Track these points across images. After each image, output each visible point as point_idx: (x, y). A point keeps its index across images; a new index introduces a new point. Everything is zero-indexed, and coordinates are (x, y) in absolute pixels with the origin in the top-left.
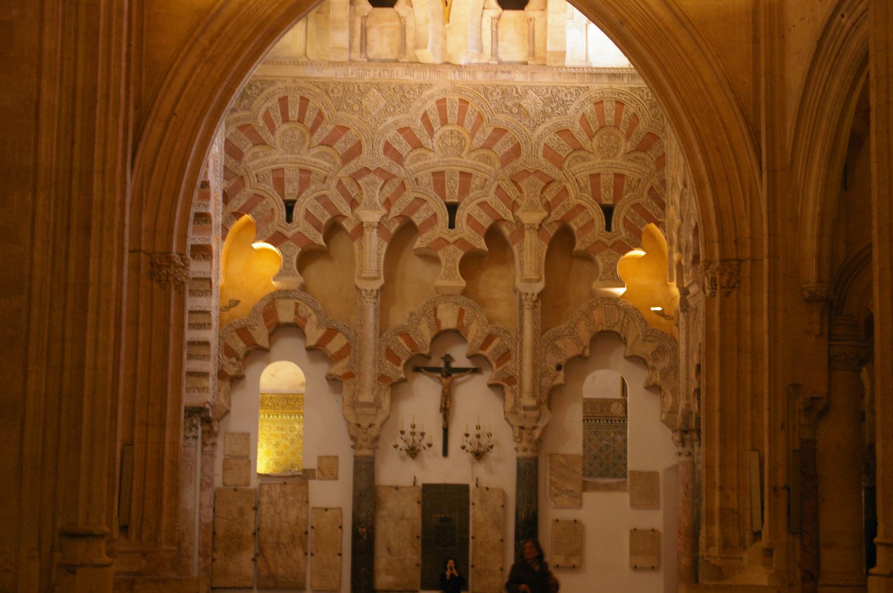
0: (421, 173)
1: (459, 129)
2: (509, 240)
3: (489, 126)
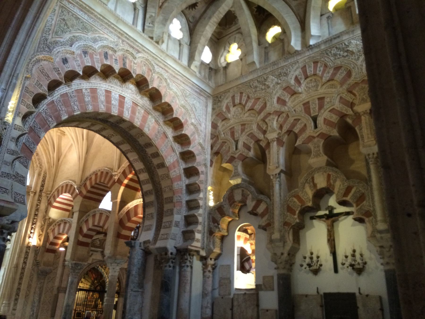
1: (315, 77)
2: (353, 125)
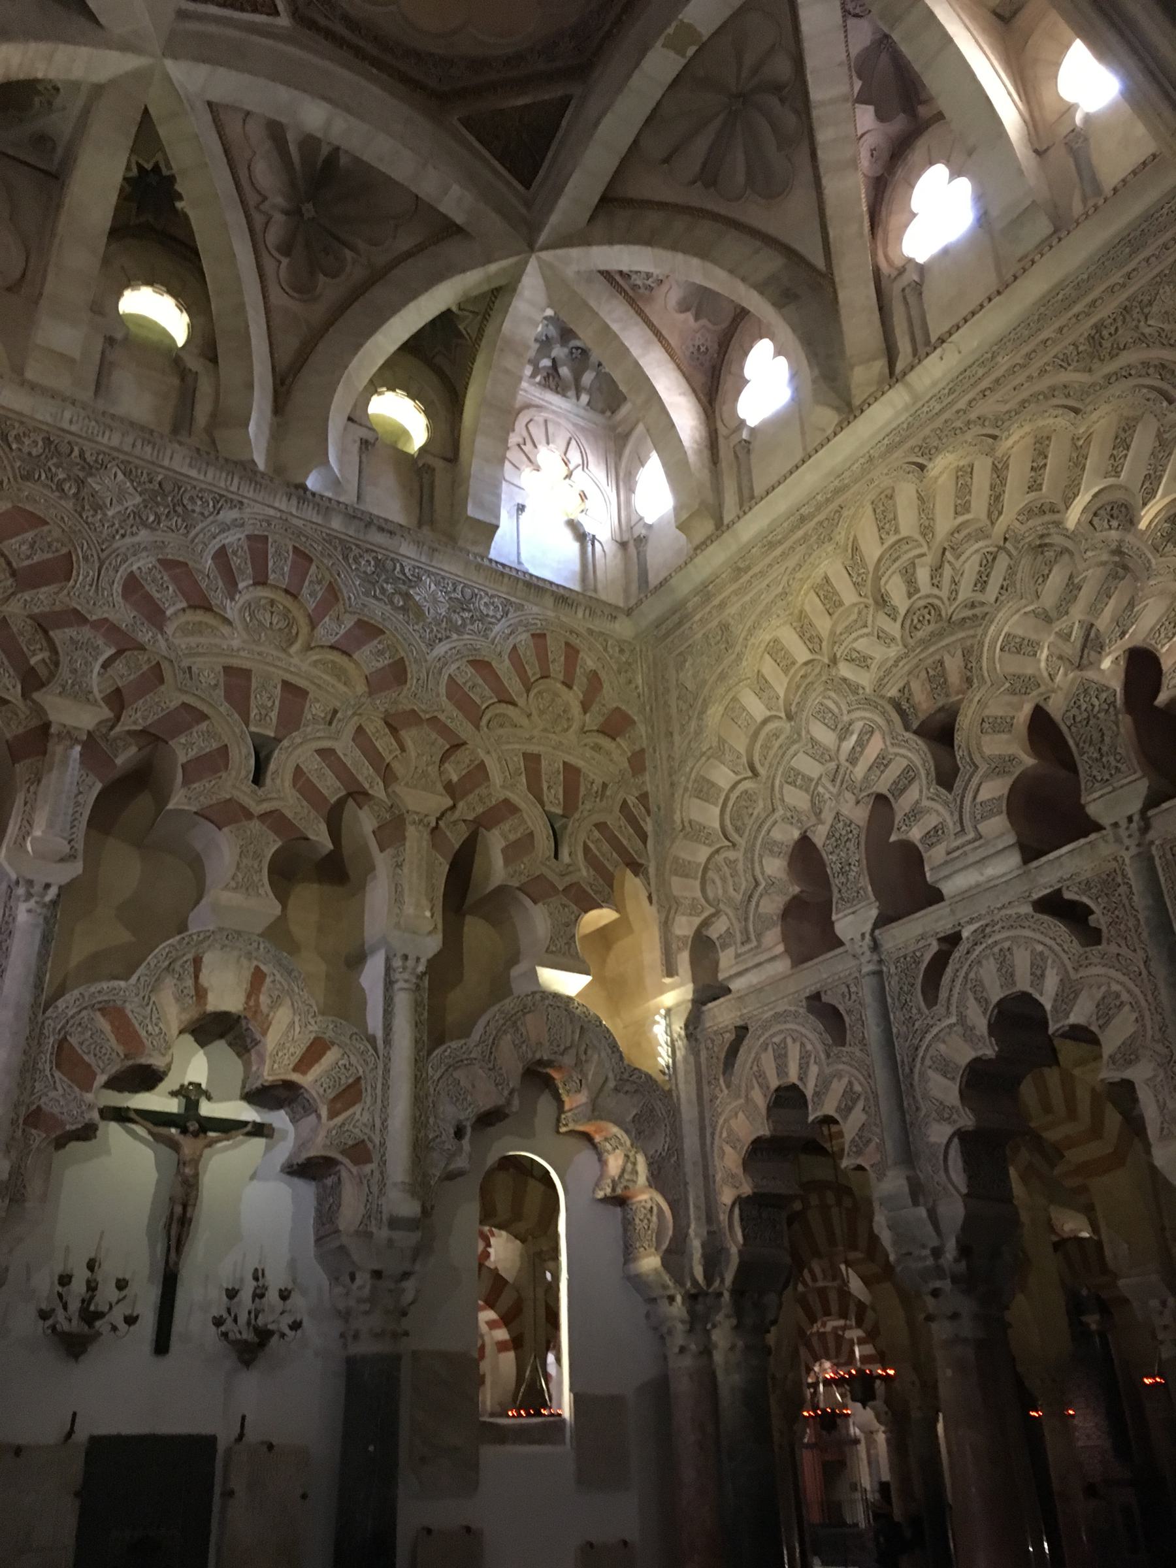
0: (198, 659)
1: (288, 602)
3: (350, 613)
